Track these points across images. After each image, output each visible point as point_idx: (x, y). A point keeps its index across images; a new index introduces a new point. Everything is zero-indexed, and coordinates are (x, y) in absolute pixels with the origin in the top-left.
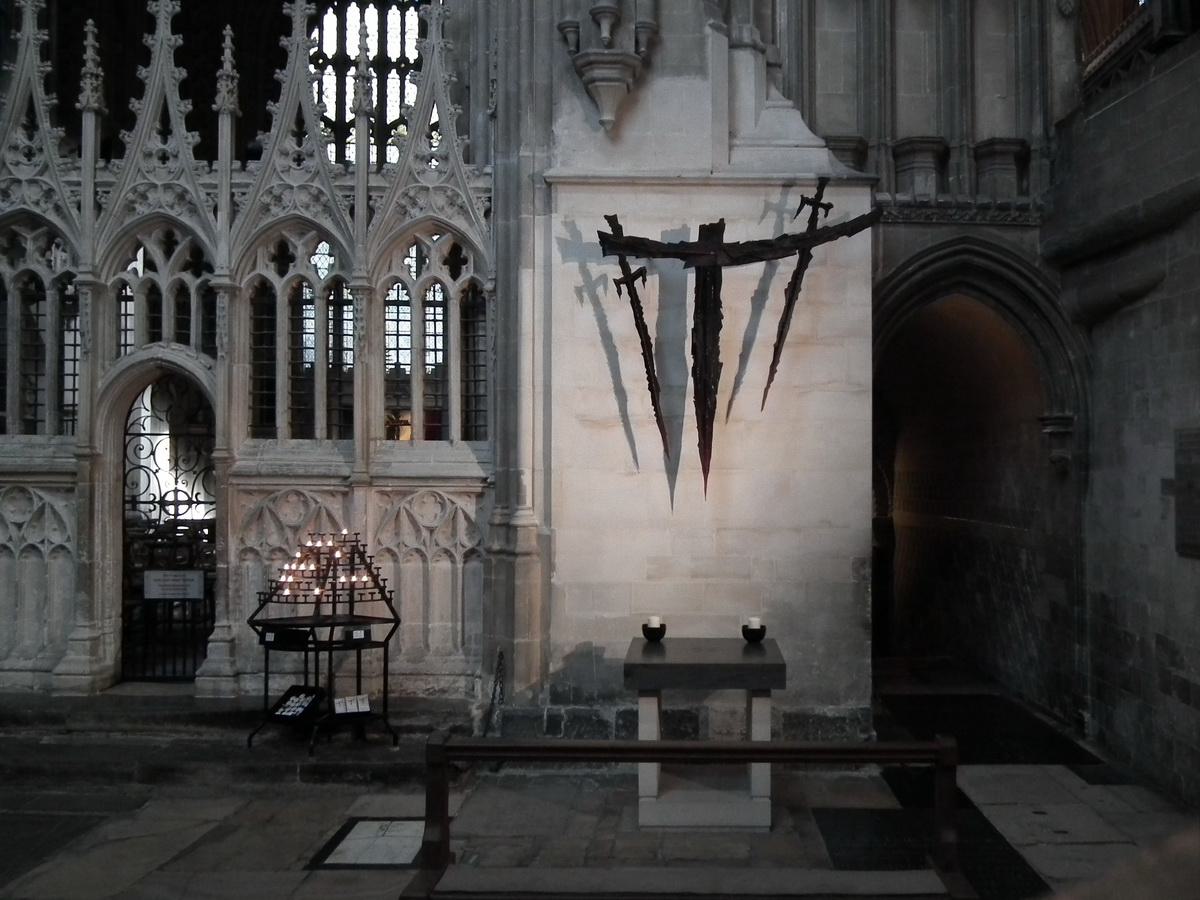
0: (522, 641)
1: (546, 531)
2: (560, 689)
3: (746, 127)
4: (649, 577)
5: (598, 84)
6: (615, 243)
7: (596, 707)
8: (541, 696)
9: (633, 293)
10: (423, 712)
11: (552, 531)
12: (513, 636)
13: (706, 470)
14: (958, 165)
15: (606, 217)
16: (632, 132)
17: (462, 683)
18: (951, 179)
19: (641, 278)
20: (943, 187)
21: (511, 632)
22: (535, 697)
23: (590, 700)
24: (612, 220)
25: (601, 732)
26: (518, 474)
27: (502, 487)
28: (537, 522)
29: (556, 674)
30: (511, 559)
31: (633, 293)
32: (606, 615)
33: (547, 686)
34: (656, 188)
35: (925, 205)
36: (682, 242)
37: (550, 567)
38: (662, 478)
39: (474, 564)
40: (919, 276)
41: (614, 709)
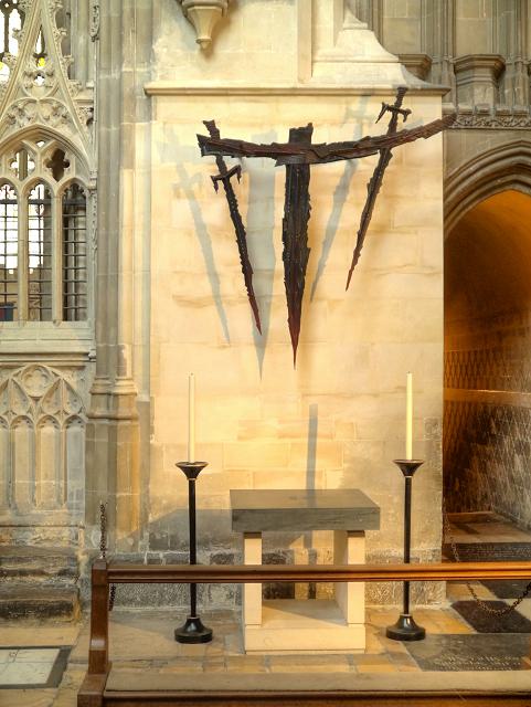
0: (124, 494)
1: (144, 398)
2: (158, 537)
3: (326, 47)
4: (240, 438)
5: (196, 8)
6: (212, 144)
8: (140, 543)
9: (228, 188)
10: (35, 558)
11: (151, 398)
12: (116, 491)
13: (295, 343)
14: (514, 79)
15: (205, 122)
16: (224, 50)
17: (66, 533)
18: (506, 91)
19: (235, 176)
20: (497, 100)
21: (113, 484)
22: (135, 544)
24: (211, 125)
26: (119, 349)
27: (106, 360)
28: (136, 390)
29: (154, 524)
30: (113, 423)
31: (228, 188)
33: (146, 534)
34: (247, 98)
35: (485, 113)
36: (274, 144)
37: (150, 430)
38: (252, 351)
39: (76, 429)
40: (479, 174)
41: (208, 554)
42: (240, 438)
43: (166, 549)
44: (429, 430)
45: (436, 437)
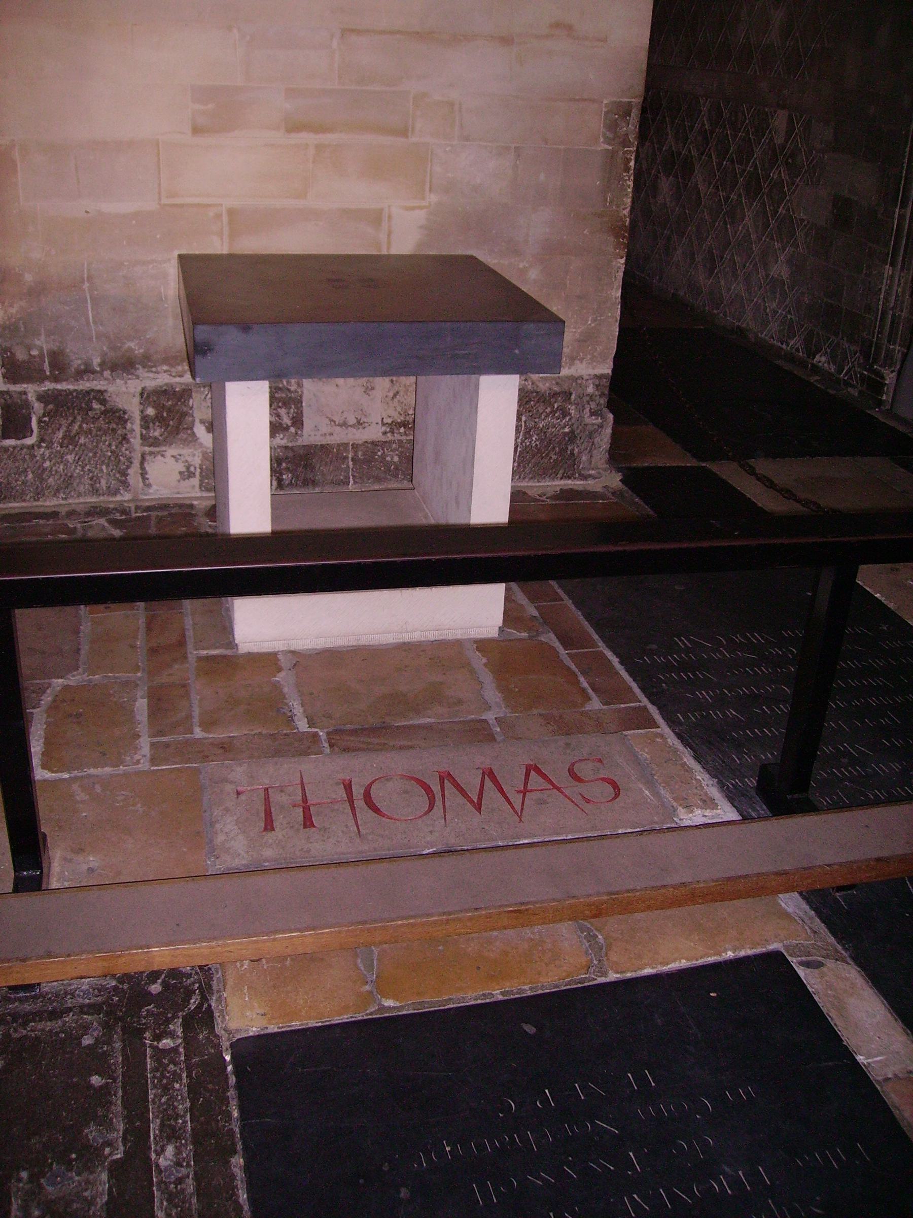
2: (21, 355)
7: (97, 385)
23: (86, 371)
25: (114, 431)
32: (111, 207)
42: (197, 130)
43: (41, 378)
44: (612, 126)
45: (625, 143)
